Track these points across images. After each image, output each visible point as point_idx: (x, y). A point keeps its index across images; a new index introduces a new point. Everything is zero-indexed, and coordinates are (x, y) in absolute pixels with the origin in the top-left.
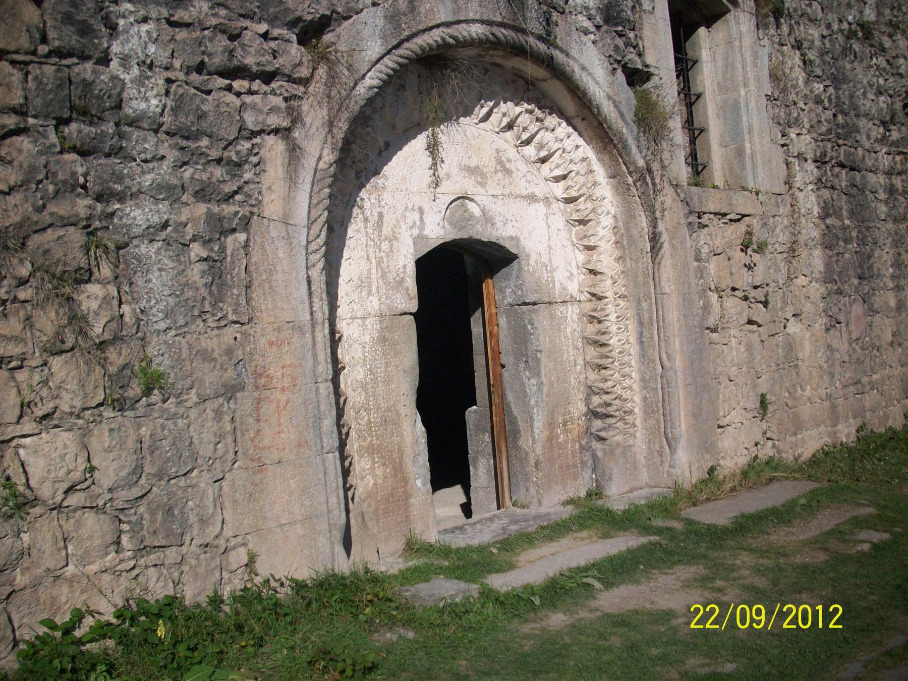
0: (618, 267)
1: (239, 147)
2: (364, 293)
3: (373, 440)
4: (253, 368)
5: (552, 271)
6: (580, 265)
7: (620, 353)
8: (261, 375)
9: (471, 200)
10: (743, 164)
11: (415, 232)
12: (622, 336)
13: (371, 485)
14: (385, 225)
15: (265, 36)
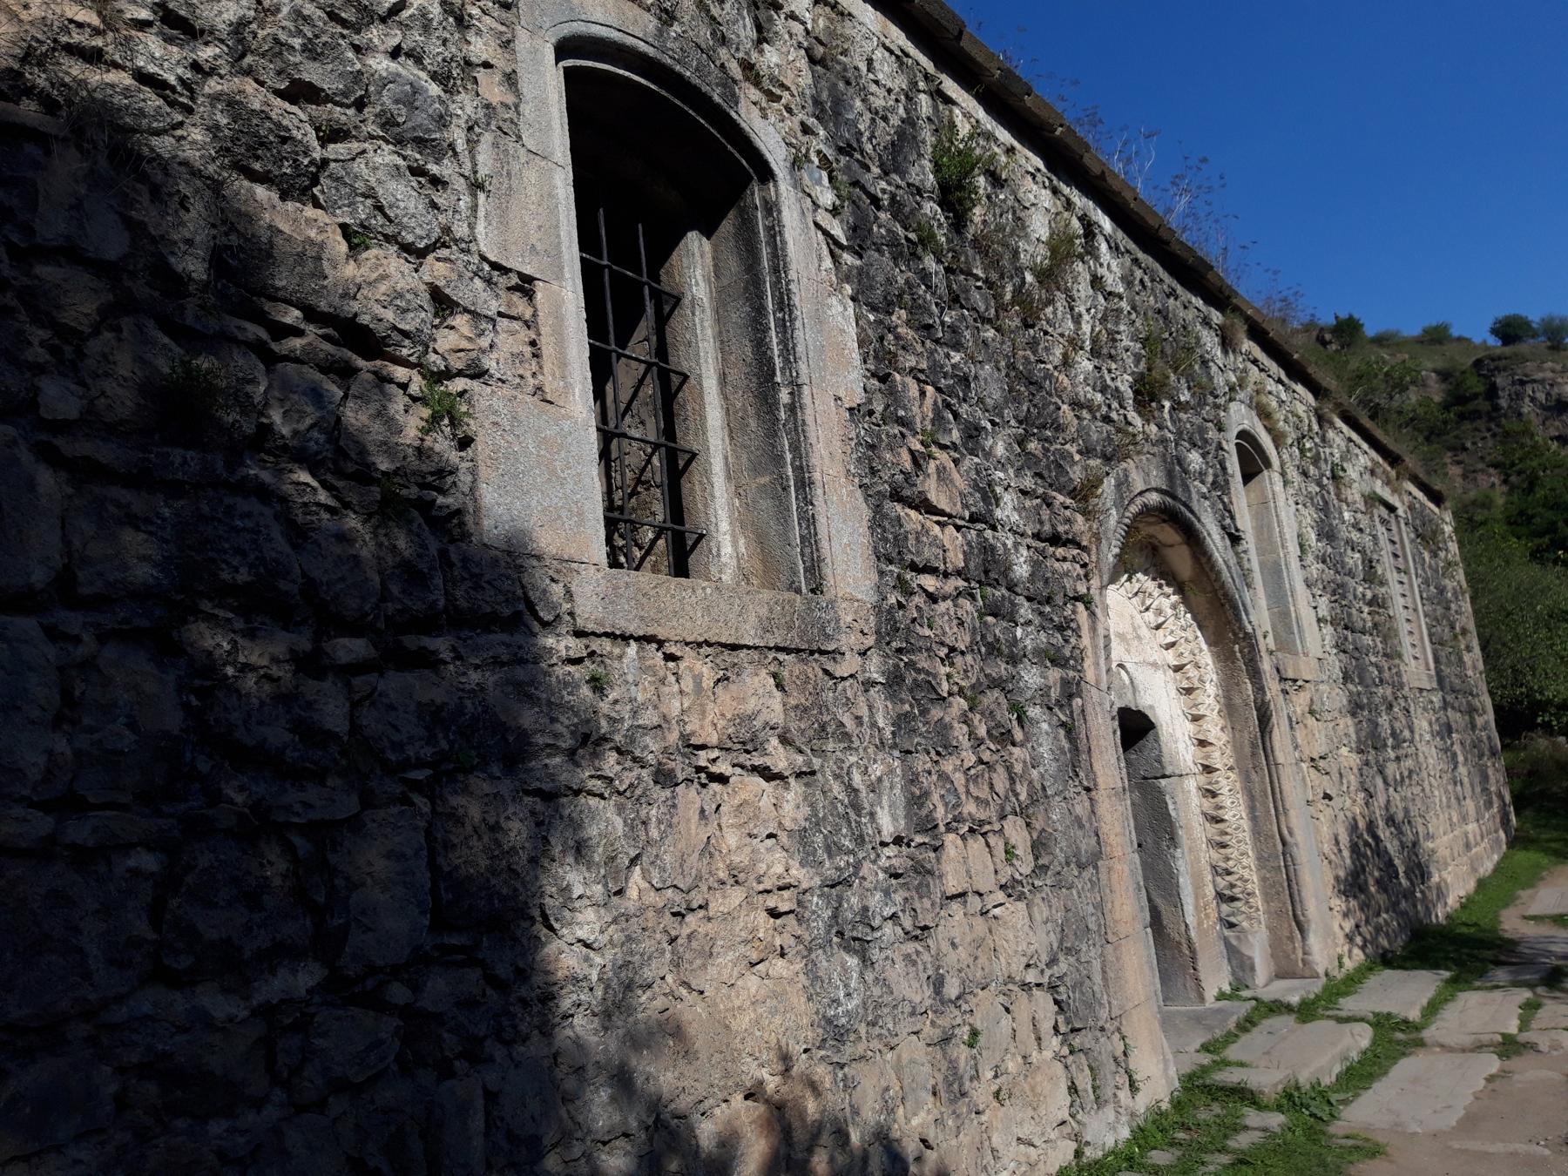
0: (1224, 737)
10: (1290, 628)
12: (1235, 810)
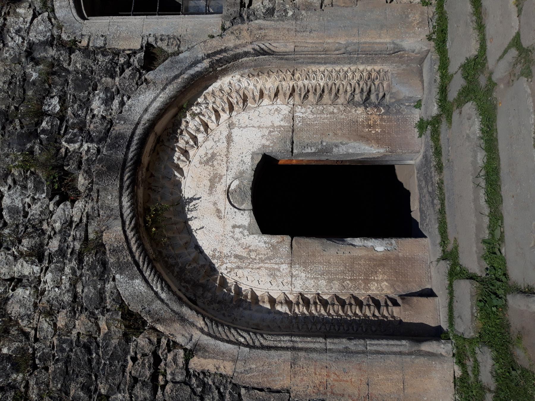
1: (195, 385)
2: (278, 274)
3: (361, 279)
4: (314, 394)
5: (273, 126)
6: (271, 103)
7: (330, 79)
8: (318, 390)
9: (229, 186)
11: (246, 232)
12: (318, 77)
13: (387, 284)
14: (241, 254)
15: (134, 359)
